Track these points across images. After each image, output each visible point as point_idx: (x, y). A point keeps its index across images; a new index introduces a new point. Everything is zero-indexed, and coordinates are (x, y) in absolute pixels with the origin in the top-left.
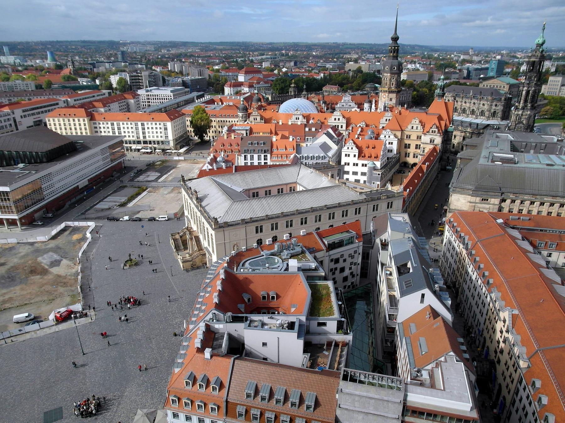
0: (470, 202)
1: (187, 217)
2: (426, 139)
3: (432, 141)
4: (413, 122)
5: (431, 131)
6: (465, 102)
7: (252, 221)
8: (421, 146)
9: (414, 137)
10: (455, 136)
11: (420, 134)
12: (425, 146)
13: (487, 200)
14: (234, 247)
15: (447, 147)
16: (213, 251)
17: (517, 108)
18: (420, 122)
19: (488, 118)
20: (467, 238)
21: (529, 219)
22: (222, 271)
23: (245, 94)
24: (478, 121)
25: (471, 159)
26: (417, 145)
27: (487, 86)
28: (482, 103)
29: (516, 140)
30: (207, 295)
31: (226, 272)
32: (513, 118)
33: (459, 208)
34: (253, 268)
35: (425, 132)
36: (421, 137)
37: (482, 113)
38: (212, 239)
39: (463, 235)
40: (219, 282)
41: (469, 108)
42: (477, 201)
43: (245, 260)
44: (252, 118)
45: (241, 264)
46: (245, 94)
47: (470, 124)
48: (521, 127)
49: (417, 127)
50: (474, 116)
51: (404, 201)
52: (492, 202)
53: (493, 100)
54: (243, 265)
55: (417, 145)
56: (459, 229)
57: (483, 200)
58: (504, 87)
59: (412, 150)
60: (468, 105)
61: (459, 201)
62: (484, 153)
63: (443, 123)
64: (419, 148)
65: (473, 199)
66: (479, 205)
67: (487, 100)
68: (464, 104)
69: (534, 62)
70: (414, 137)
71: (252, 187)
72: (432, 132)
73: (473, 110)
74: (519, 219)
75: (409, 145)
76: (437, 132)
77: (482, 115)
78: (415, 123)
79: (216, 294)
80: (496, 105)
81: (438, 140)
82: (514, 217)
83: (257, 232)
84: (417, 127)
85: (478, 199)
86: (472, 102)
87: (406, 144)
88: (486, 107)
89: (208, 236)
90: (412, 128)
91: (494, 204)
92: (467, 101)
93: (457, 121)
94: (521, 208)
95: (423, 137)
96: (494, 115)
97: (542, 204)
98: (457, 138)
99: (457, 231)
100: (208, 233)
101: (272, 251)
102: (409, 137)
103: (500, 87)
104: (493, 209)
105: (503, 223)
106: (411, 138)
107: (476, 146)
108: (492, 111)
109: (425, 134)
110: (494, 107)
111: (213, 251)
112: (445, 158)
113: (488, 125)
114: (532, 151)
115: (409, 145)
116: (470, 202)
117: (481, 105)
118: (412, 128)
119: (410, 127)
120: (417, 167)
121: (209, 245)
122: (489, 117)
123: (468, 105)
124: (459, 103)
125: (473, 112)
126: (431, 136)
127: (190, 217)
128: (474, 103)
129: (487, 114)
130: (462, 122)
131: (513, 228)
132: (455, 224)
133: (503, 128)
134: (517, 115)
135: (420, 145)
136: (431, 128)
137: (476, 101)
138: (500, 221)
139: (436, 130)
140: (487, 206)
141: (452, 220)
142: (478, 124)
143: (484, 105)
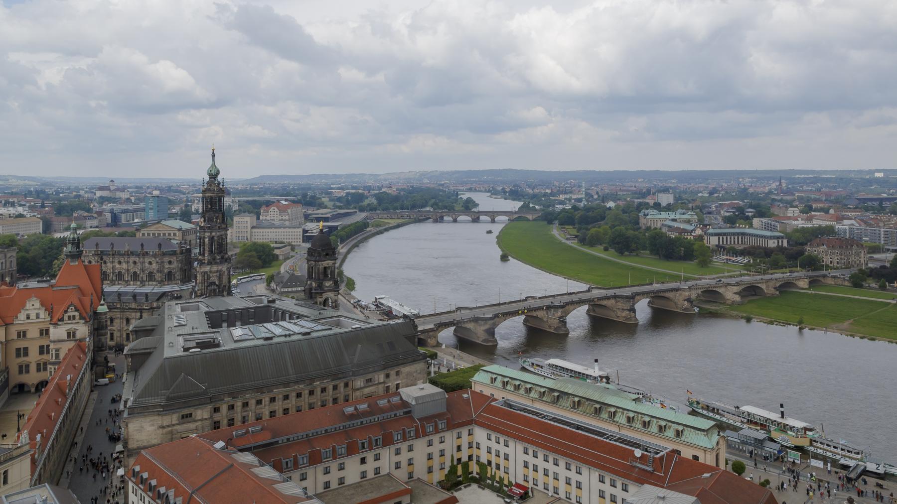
0: (163, 427)
2: (58, 332)
3: (71, 335)
4: (29, 305)
5: (66, 318)
6: (120, 263)
8: (52, 346)
9: (33, 333)
10: (112, 320)
11: (43, 326)
12: (58, 346)
13: (191, 415)
15: (100, 340)
17: (201, 263)
18: (42, 304)
19: (161, 283)
20: (171, 494)
21: (262, 429)
24: (147, 289)
25: (150, 353)
26: (41, 347)
27: (149, 234)
28: (147, 260)
29: (211, 310)
32: (199, 278)
33: (145, 444)
35: (55, 320)
36: (47, 331)
37: (151, 277)
39: (162, 490)
41: (128, 270)
42: (174, 422)
47: (135, 296)
48: (215, 290)
49: (38, 316)
50: (139, 283)
51: (34, 462)
52: (199, 418)
53: (164, 254)
55: (41, 348)
56: (154, 482)
57: (183, 417)
58: (175, 235)
59: (34, 357)
60: (125, 266)
61: (143, 431)
62: (168, 338)
63: (87, 300)
64: (48, 352)
65: (167, 420)
66: (179, 428)
67: (155, 256)
68: (118, 266)
69: (211, 197)
70: (33, 333)
72: (69, 318)
73: (135, 273)
74: (247, 432)
75: (26, 349)
76: (77, 318)
77: (151, 280)
78: (33, 307)
80: (170, 262)
81: (83, 330)
82: (239, 432)
84: (38, 316)
85: (174, 418)
86: (131, 262)
87: (18, 350)
88: (155, 266)
90: (28, 318)
91: (202, 420)
92: (122, 260)
93: (111, 293)
94: (245, 414)
95: (52, 330)
96: (170, 277)
97: (273, 400)
98: (117, 322)
99: (151, 488)
102: (22, 335)
103: (169, 234)
104: (203, 429)
105: (223, 448)
106: (29, 335)
107: (153, 330)
108: (166, 271)
109: (55, 325)
110: (167, 266)
112: (101, 359)
113: (164, 294)
114: (238, 323)
115: (26, 349)
116: (163, 427)
117: (147, 265)
118: (28, 318)
119: (22, 316)
120: (51, 387)
122: (162, 281)
123: (125, 266)
124: (109, 265)
125: (135, 277)
126: (68, 327)
128: (135, 263)
129: (158, 276)
130: (119, 294)
131: (242, 450)
132: (145, 475)
133: (186, 294)
134: (205, 273)
135: (48, 346)
136: (66, 312)
137: (137, 259)
138: (220, 444)
139: (76, 314)
140: (192, 426)
141: (137, 469)
142: (147, 295)
143: (150, 263)
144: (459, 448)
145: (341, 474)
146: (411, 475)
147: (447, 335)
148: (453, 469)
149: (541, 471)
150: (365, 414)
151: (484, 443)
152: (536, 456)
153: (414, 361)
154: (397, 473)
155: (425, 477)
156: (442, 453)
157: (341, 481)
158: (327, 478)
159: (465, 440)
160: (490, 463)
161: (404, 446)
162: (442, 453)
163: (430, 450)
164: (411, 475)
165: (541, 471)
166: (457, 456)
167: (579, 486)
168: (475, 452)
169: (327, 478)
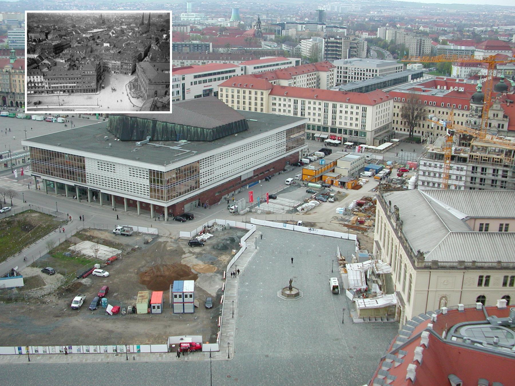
1: (377, 242)
7: (474, 266)
14: (441, 299)
16: (409, 300)
22: (425, 334)
23: (483, 77)
30: (397, 364)
31: (431, 337)
34: (472, 339)
38: (411, 282)
40: (419, 350)
43: (461, 324)
44: (490, 114)
45: (453, 330)
46: (483, 77)
54: (456, 331)
71: (481, 215)
79: (412, 367)
83: (480, 284)
89: (405, 276)
100: (405, 272)
101: (505, 319)
111: (409, 300)
121: (404, 290)
127: (381, 244)
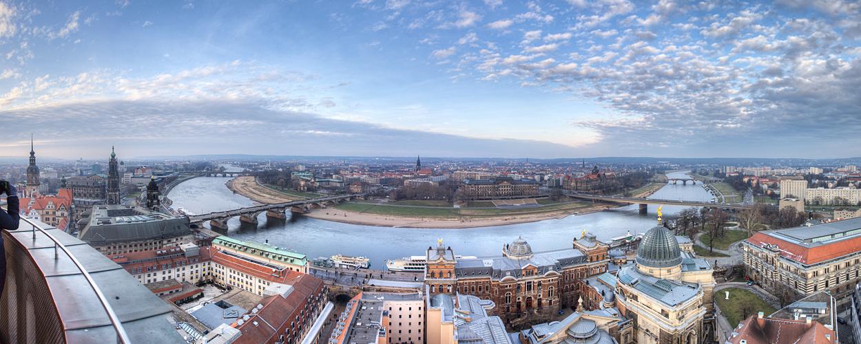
144: (204, 270)
145: (155, 277)
146: (184, 280)
147: (207, 224)
148: (201, 278)
149: (236, 279)
150: (165, 254)
151: (215, 268)
152: (234, 273)
153: (188, 234)
154: (178, 279)
155: (190, 281)
156: (197, 272)
157: (155, 280)
158: (149, 278)
159: (207, 267)
160: (217, 276)
161: (181, 268)
162: (197, 272)
163: (192, 270)
164: (184, 280)
165: (236, 279)
166: (203, 273)
167: (251, 284)
168: (211, 271)
169: (149, 278)
